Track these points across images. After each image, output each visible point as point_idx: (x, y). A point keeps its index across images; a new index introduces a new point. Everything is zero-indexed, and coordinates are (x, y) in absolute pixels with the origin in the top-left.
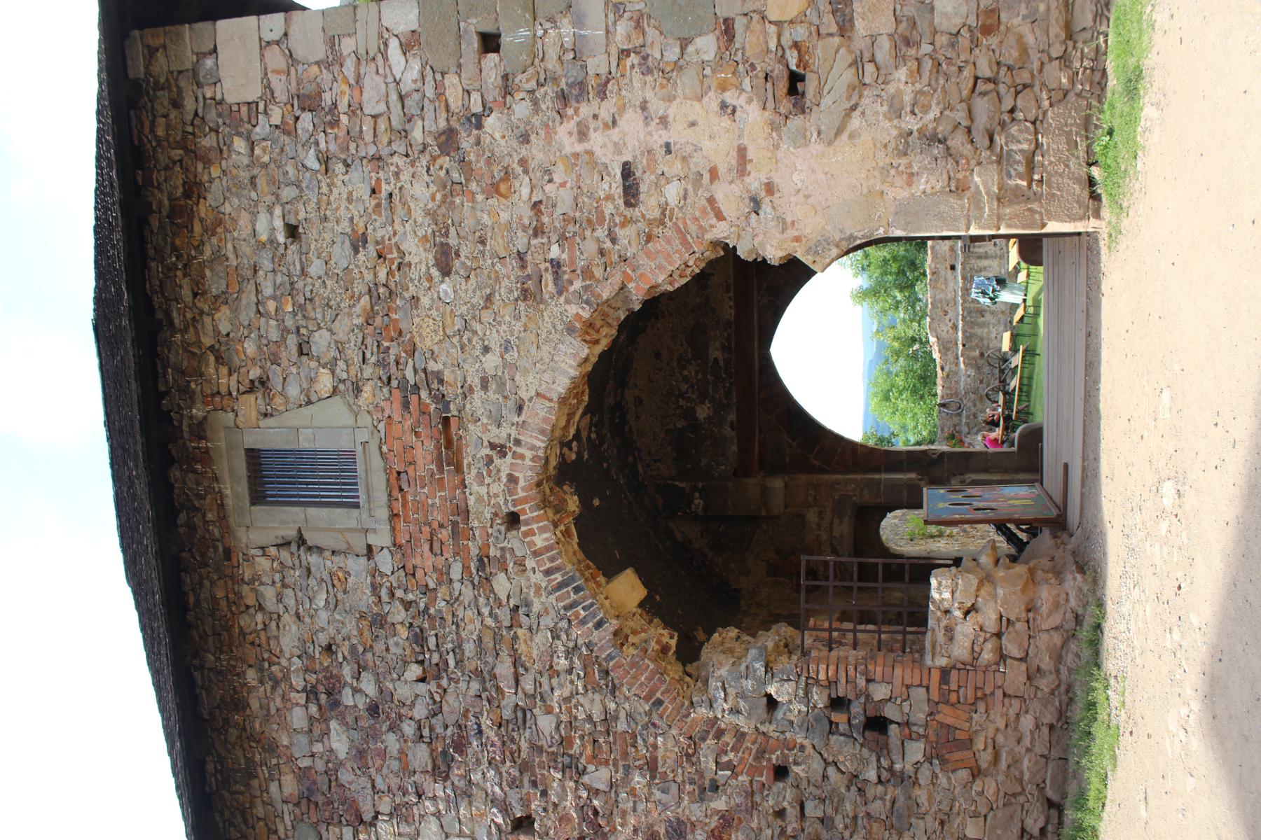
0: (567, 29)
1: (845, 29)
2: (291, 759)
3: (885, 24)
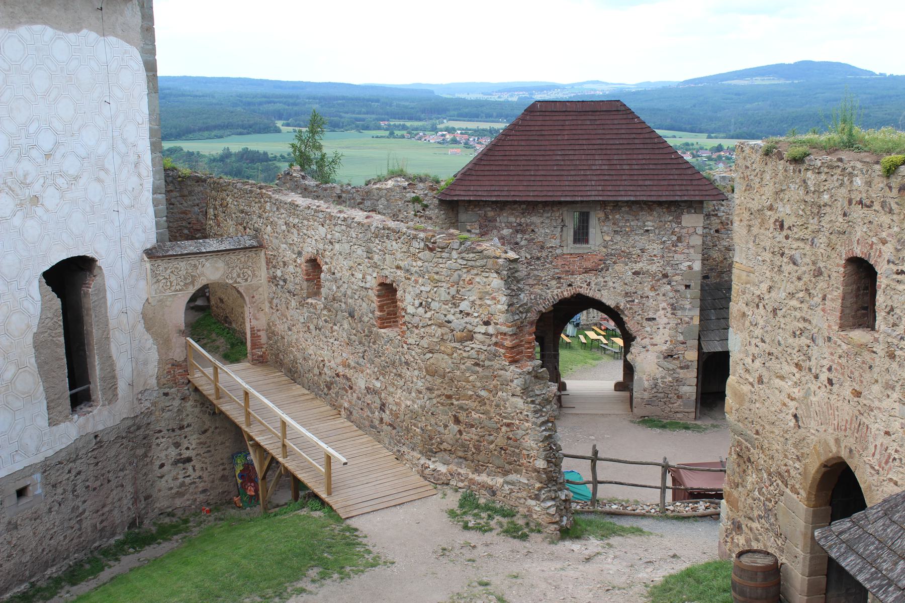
0: (688, 306)
1: (681, 368)
2: (499, 216)
3: (681, 376)
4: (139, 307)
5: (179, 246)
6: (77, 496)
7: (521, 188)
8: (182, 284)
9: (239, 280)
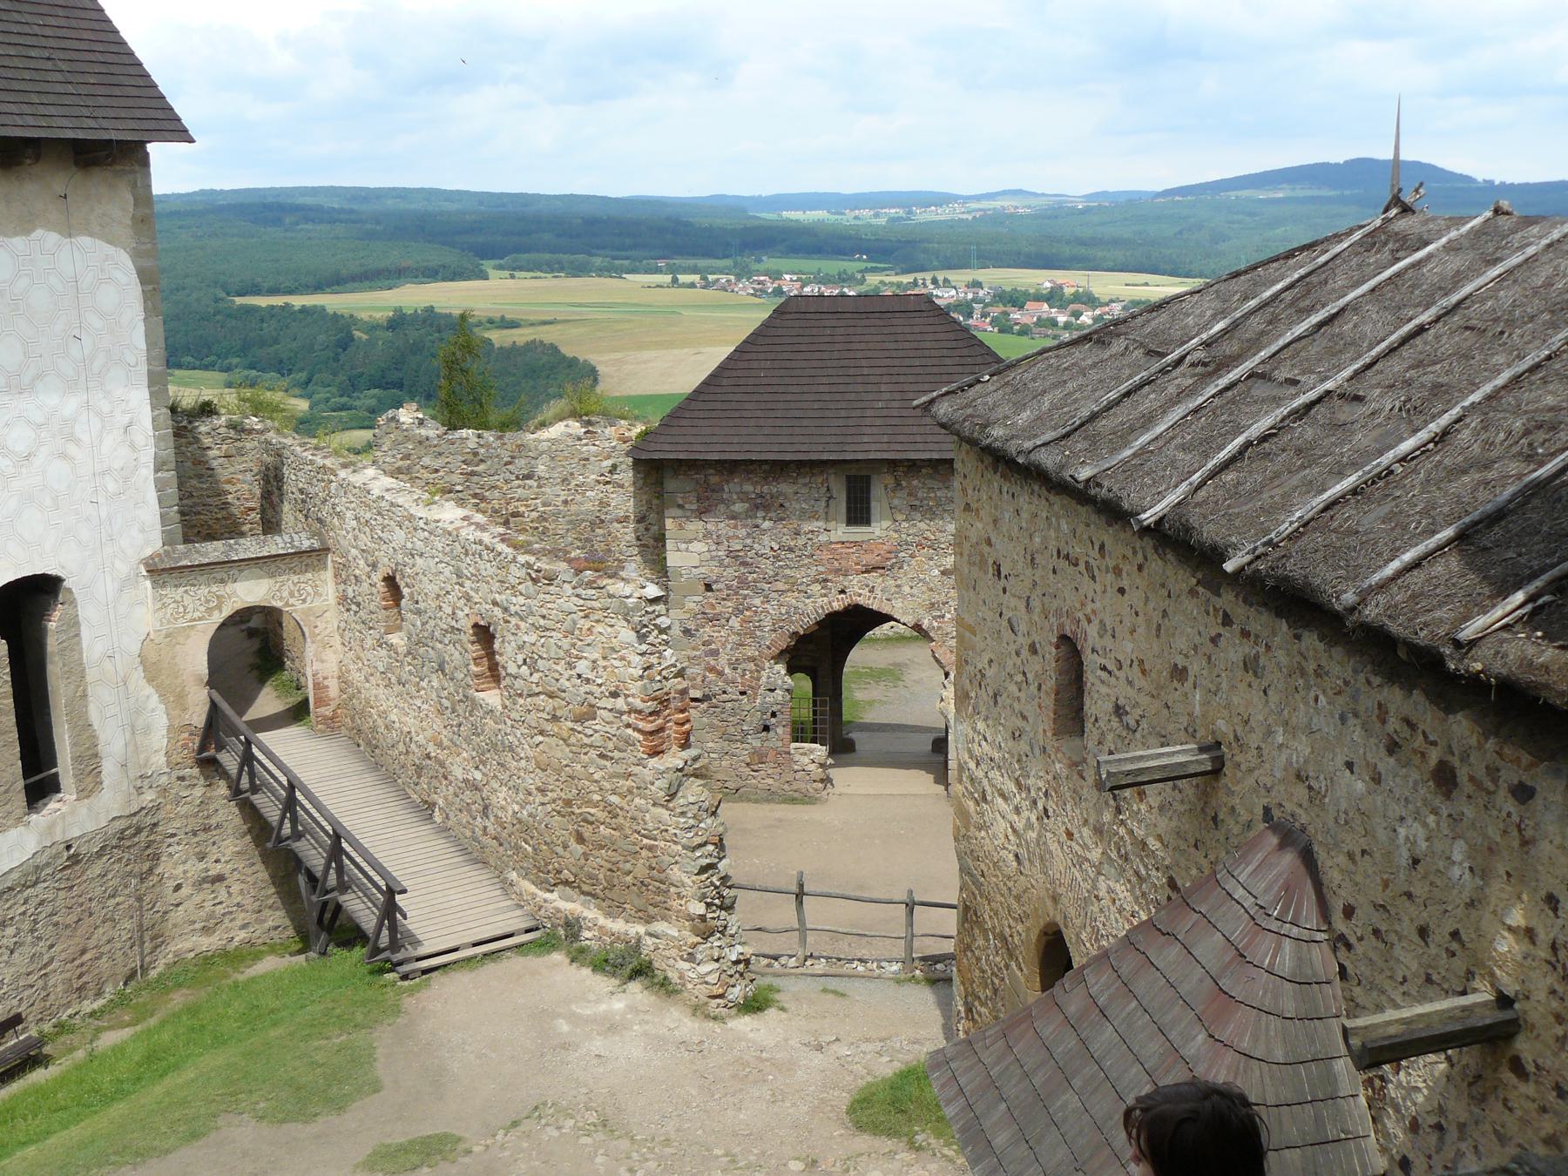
2: (728, 482)
4: (135, 649)
5: (198, 552)
6: (39, 939)
7: (761, 439)
8: (202, 609)
9: (291, 601)
